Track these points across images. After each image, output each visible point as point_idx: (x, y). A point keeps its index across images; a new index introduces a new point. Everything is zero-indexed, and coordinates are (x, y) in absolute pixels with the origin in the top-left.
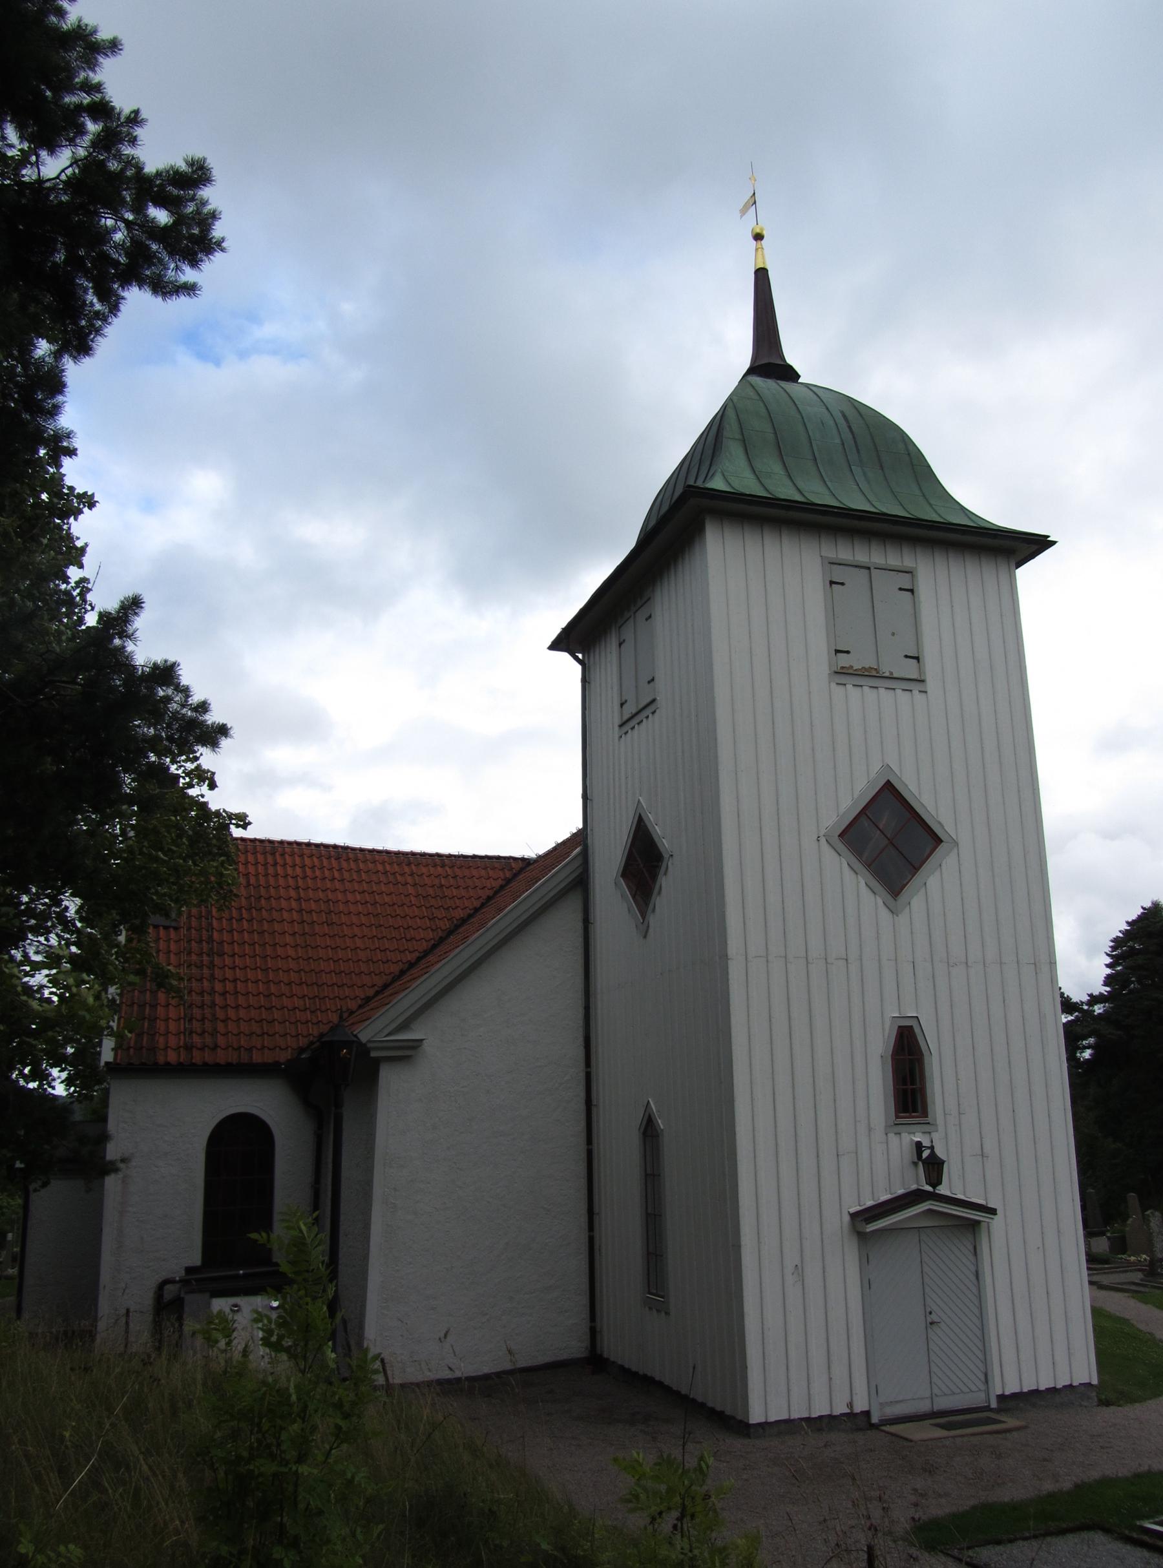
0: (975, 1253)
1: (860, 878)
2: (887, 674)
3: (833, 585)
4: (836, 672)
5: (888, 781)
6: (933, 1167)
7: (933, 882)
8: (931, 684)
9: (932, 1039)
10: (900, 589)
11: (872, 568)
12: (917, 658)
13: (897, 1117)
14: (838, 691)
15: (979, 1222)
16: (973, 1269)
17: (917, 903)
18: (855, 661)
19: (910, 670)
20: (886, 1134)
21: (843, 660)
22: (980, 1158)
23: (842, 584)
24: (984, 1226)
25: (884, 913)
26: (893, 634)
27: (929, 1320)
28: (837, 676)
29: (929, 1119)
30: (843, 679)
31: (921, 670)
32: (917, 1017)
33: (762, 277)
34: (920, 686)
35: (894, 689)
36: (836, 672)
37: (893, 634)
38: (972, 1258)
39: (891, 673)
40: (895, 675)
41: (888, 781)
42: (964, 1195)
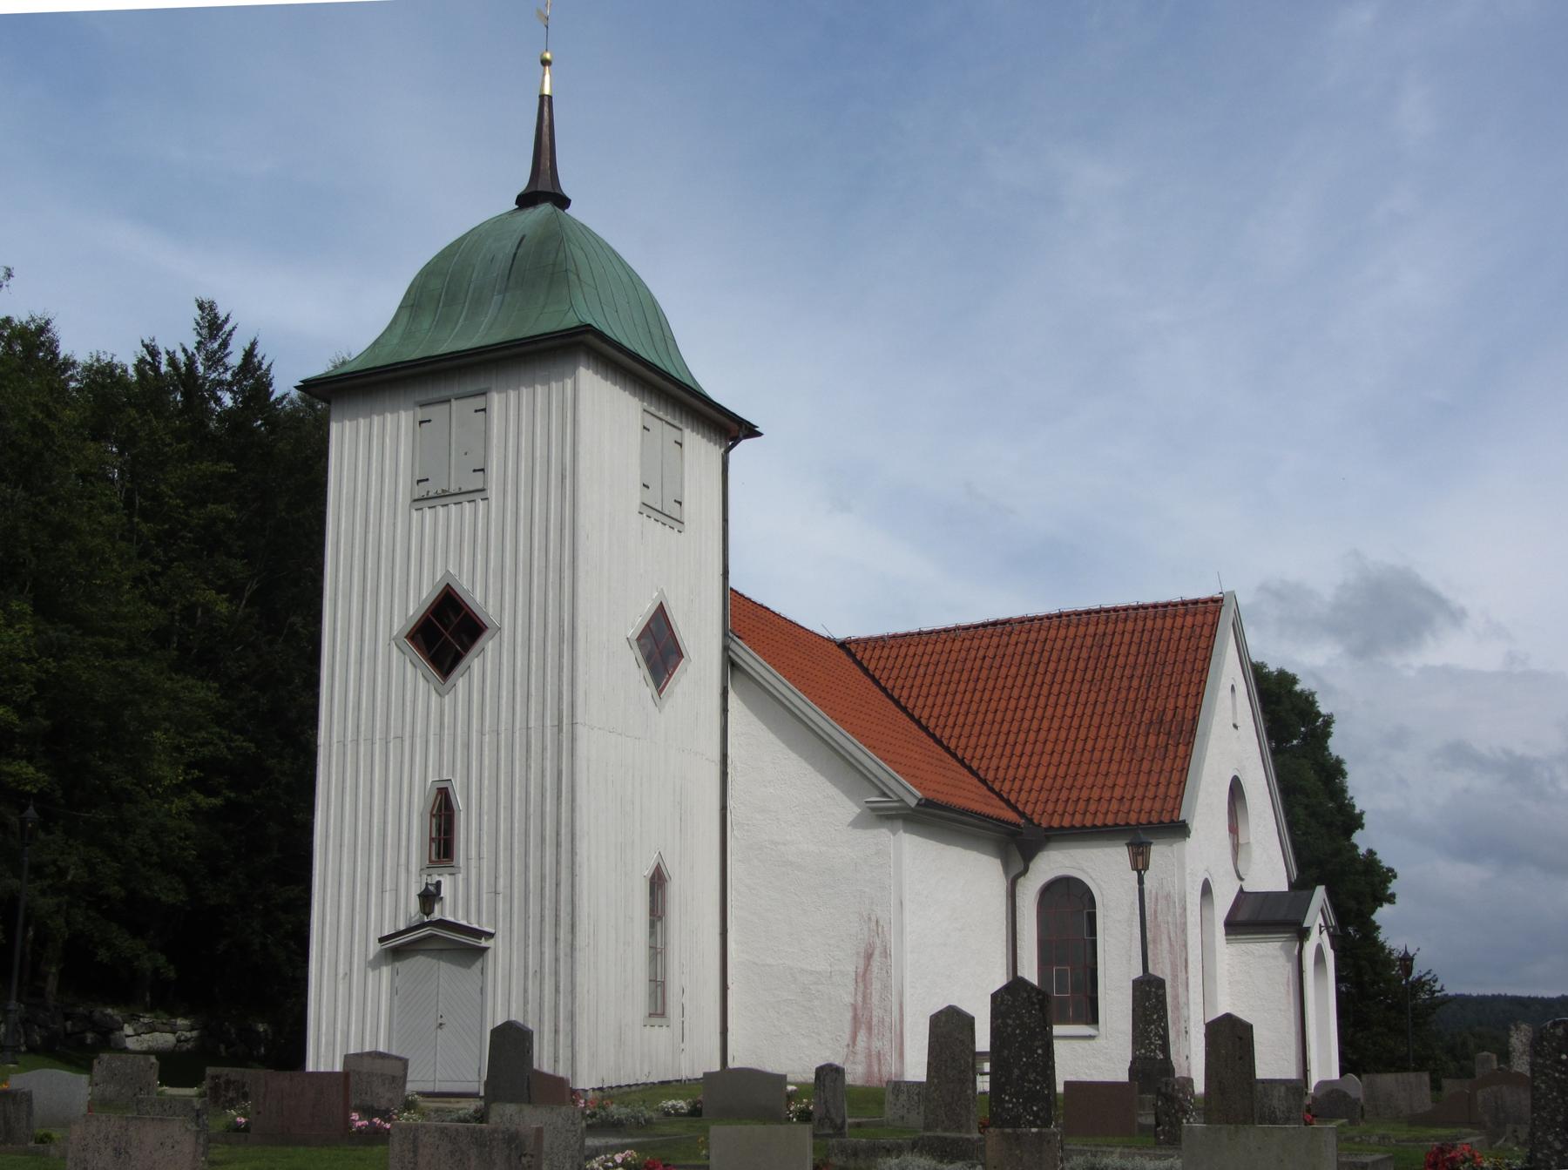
0: (482, 973)
1: (419, 671)
2: (457, 491)
3: (423, 425)
4: (415, 500)
5: (448, 584)
6: (429, 898)
7: (476, 664)
8: (493, 492)
9: (459, 800)
10: (476, 411)
11: (453, 400)
12: (483, 470)
13: (430, 861)
14: (415, 514)
15: (485, 949)
16: (480, 985)
17: (461, 684)
18: (432, 488)
19: (475, 482)
20: (421, 876)
21: (420, 491)
22: (493, 894)
23: (429, 421)
24: (490, 953)
25: (434, 695)
26: (466, 454)
27: (440, 1021)
28: (416, 503)
29: (454, 863)
30: (419, 504)
31: (485, 482)
32: (450, 780)
33: (545, 102)
34: (482, 495)
35: (461, 503)
36: (415, 500)
37: (466, 454)
38: (481, 977)
39: (460, 489)
40: (463, 490)
41: (448, 584)
42: (479, 923)
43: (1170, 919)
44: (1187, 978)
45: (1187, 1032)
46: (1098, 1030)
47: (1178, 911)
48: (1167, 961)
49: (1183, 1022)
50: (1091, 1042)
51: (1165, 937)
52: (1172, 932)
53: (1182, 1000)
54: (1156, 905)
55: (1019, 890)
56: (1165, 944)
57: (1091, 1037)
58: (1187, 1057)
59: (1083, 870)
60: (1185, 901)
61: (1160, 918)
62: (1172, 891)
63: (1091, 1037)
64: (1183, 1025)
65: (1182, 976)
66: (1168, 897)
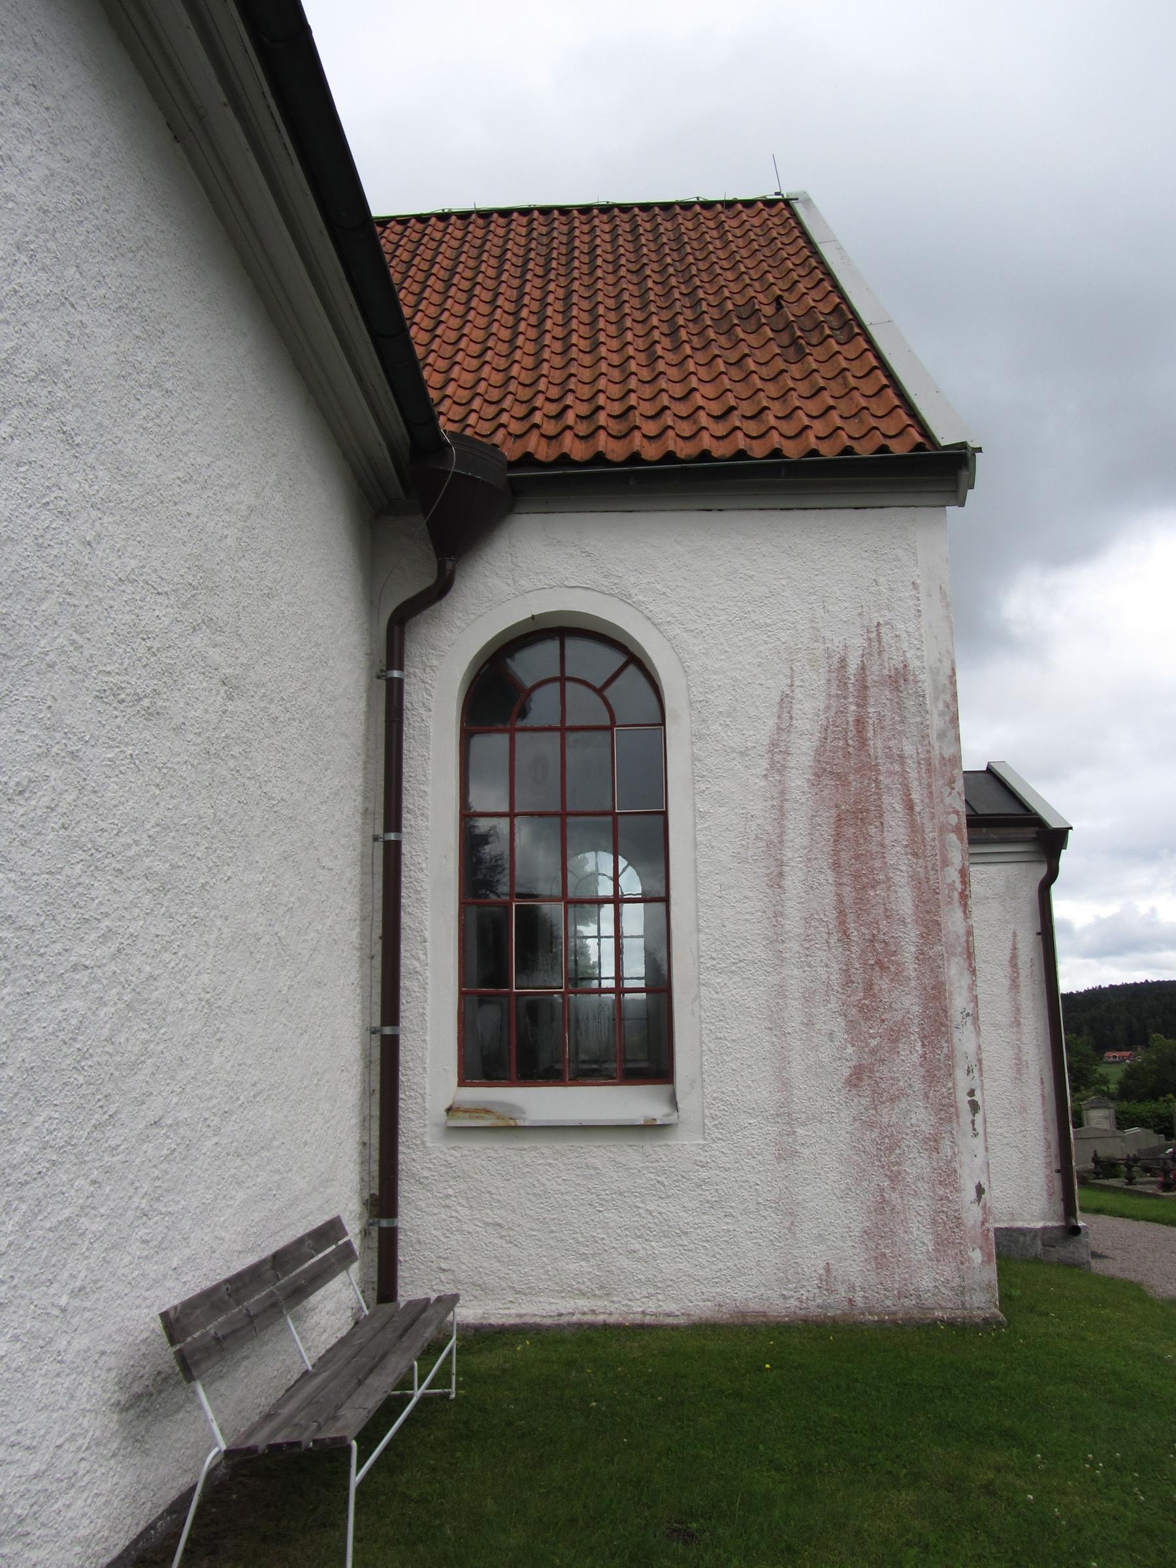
43: (909, 749)
44: (969, 933)
45: (974, 1107)
46: (673, 1102)
47: (936, 722)
48: (901, 878)
49: (960, 1074)
50: (654, 1148)
51: (893, 802)
52: (914, 784)
53: (959, 1002)
54: (862, 704)
55: (414, 652)
56: (896, 828)
57: (651, 1129)
58: (980, 1190)
59: (625, 598)
60: (955, 696)
61: (876, 745)
62: (914, 664)
63: (651, 1129)
64: (962, 1082)
65: (953, 921)
66: (899, 679)
